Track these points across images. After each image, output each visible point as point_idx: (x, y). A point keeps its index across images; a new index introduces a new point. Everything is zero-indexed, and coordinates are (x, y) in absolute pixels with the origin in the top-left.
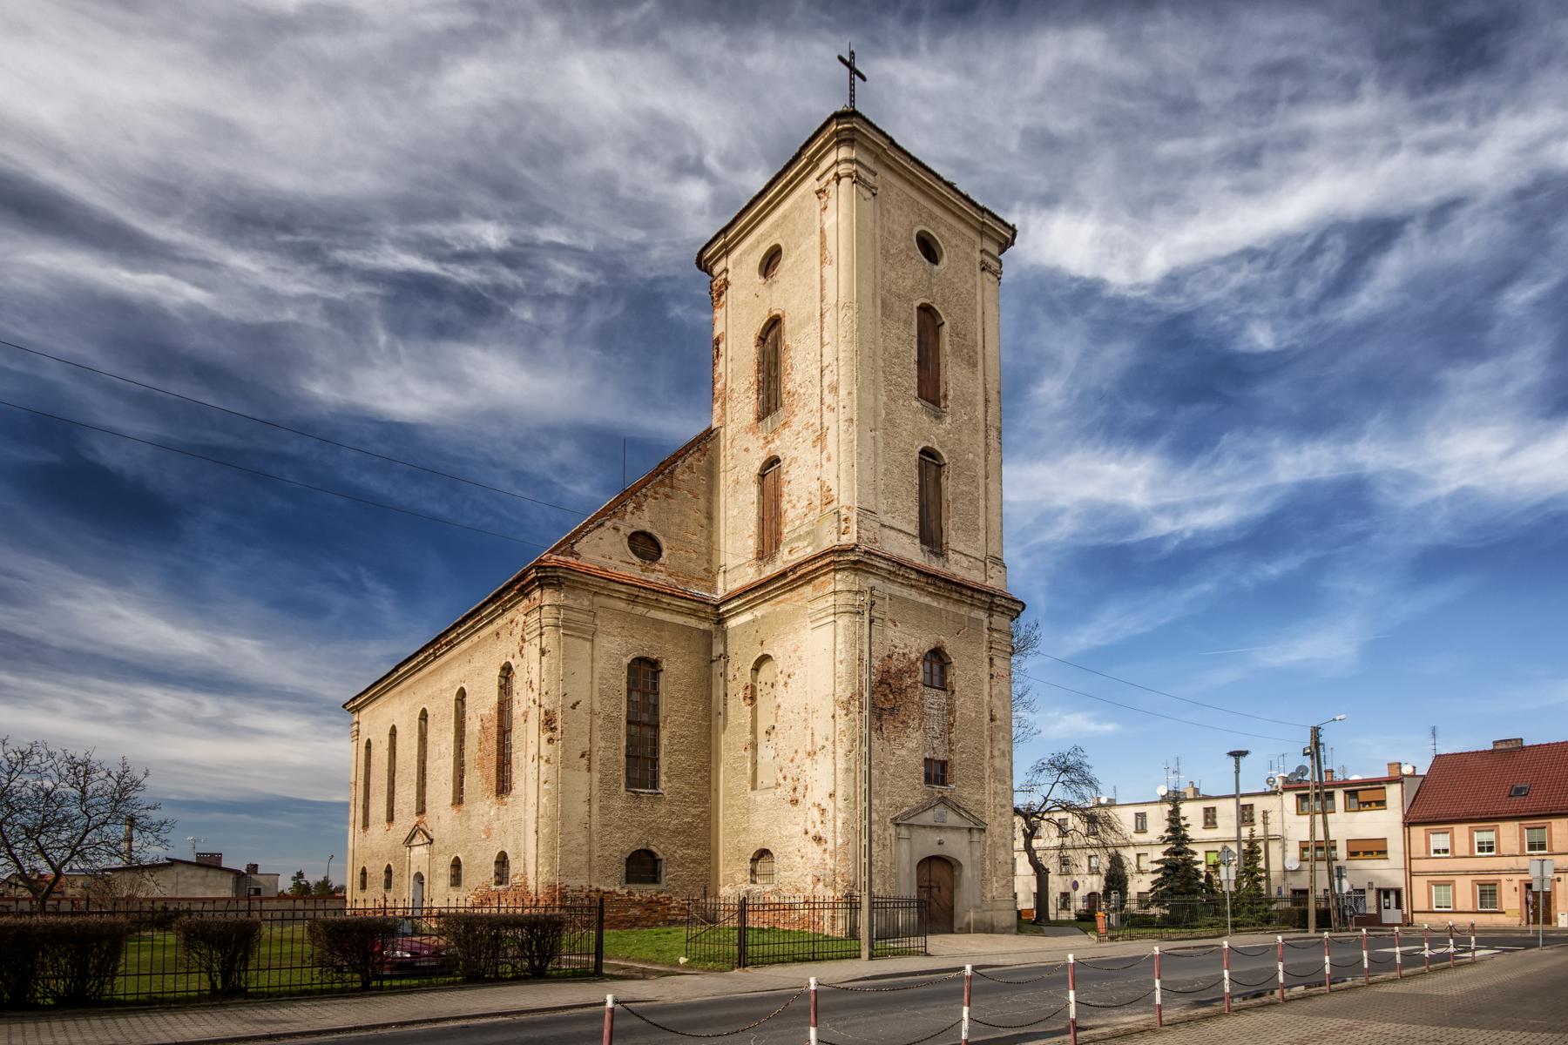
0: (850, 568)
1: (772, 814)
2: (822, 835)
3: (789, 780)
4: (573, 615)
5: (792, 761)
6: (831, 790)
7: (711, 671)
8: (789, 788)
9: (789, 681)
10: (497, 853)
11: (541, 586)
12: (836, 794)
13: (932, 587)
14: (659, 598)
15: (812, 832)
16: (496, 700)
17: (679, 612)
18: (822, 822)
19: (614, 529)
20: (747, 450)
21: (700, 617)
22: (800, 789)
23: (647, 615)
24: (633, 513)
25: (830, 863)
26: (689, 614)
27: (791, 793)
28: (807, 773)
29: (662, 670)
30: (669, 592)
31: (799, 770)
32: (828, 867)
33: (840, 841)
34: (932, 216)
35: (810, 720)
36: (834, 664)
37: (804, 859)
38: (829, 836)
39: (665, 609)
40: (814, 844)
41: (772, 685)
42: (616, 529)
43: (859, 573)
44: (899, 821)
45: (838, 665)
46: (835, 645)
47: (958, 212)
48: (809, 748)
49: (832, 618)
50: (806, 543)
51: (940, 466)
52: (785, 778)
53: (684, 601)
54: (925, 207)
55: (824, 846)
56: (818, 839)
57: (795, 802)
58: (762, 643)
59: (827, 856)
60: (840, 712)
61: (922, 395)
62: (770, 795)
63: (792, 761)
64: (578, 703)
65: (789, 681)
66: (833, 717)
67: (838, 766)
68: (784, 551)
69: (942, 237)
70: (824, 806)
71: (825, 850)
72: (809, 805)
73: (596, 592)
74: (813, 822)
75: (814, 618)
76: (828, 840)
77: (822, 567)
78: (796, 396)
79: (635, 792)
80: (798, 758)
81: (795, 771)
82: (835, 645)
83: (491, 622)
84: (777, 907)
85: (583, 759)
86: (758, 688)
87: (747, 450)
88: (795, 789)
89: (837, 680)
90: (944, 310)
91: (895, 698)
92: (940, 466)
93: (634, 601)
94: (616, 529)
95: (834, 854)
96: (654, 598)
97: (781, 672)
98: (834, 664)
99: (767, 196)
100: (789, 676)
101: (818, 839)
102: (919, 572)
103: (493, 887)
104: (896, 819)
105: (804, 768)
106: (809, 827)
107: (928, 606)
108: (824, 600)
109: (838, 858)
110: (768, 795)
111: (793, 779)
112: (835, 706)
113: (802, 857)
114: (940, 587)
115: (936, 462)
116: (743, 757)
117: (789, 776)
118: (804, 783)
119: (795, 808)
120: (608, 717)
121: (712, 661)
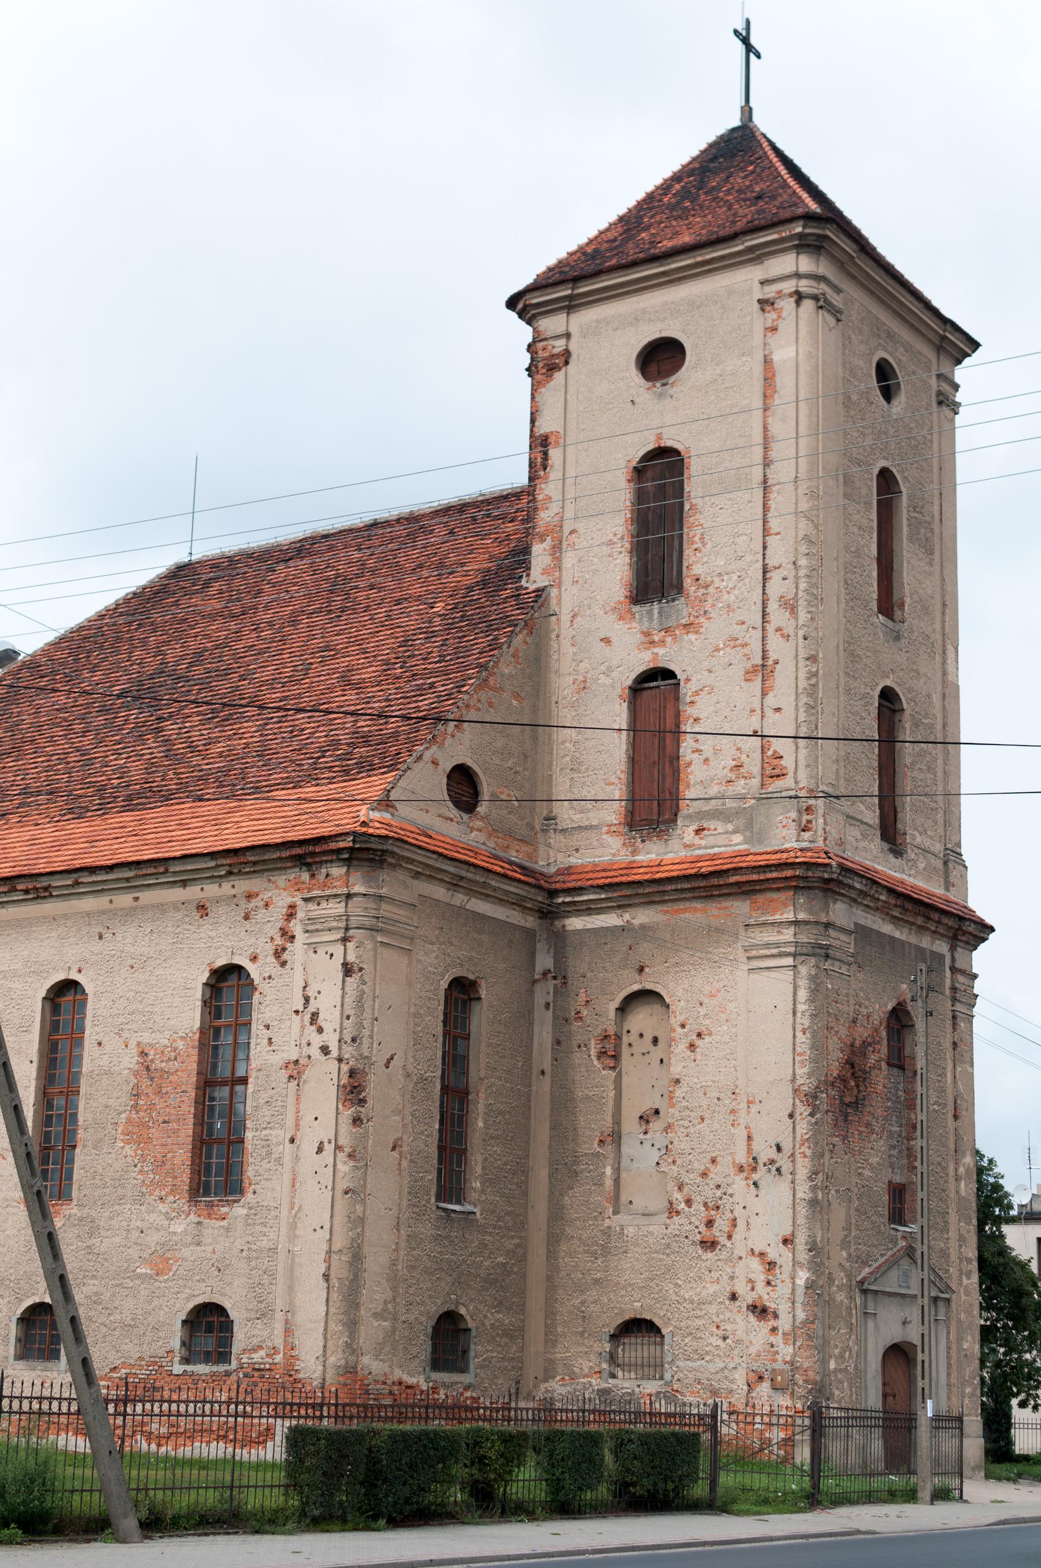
0: (818, 888)
1: (660, 1260)
2: (768, 1304)
3: (698, 1207)
4: (387, 910)
5: (704, 1175)
6: (787, 1231)
7: (533, 998)
8: (699, 1221)
9: (698, 1042)
10: (190, 1305)
11: (348, 862)
12: (797, 1241)
13: (899, 910)
14: (488, 881)
15: (748, 1297)
16: (197, 1024)
17: (503, 900)
18: (769, 1283)
19: (433, 762)
20: (607, 641)
21: (526, 908)
22: (721, 1224)
23: (467, 907)
24: (453, 736)
25: (786, 1351)
26: (514, 904)
27: (702, 1228)
28: (736, 1199)
29: (479, 999)
30: (499, 869)
31: (719, 1193)
32: (779, 1358)
33: (801, 1315)
34: (890, 335)
35: (743, 1113)
36: (794, 1036)
37: (729, 1341)
38: (783, 1308)
39: (488, 896)
40: (752, 1318)
41: (655, 1041)
42: (435, 763)
43: (829, 894)
44: (866, 1286)
45: (799, 1034)
46: (795, 1004)
47: (917, 325)
48: (742, 1158)
49: (790, 961)
50: (730, 827)
51: (894, 711)
52: (689, 1202)
53: (515, 884)
54: (884, 324)
55: (772, 1323)
56: (760, 1311)
57: (710, 1245)
58: (641, 970)
59: (778, 1340)
60: (802, 1110)
61: (881, 611)
62: (656, 1228)
63: (704, 1175)
64: (392, 1058)
65: (698, 1042)
66: (791, 1116)
67: (800, 1195)
68: (685, 832)
69: (899, 363)
70: (772, 1255)
71: (774, 1330)
72: (740, 1250)
73: (418, 873)
74: (750, 1281)
75: (754, 953)
76: (780, 1313)
77: (774, 880)
78: (711, 590)
79: (445, 1210)
80: (716, 1175)
81: (709, 1193)
82: (795, 1004)
83: (184, 883)
84: (774, 1420)
85: (393, 1153)
86: (625, 1039)
87: (607, 641)
88: (710, 1223)
89: (798, 1058)
90: (902, 472)
91: (857, 1086)
92: (894, 711)
93: (456, 885)
94: (435, 763)
95: (791, 1336)
96: (482, 880)
97: (683, 1026)
98: (794, 1036)
99: (668, 264)
100: (699, 1035)
101: (760, 1311)
102: (891, 891)
103: (178, 1369)
104: (862, 1282)
105: (730, 1191)
106: (741, 1289)
107: (892, 939)
108: (776, 929)
109: (798, 1343)
110: (651, 1228)
111: (705, 1205)
112: (794, 1099)
113: (725, 1338)
114: (907, 910)
115: (888, 705)
116: (597, 1155)
117: (698, 1199)
118: (729, 1215)
119: (710, 1255)
120: (422, 1079)
121: (535, 982)
